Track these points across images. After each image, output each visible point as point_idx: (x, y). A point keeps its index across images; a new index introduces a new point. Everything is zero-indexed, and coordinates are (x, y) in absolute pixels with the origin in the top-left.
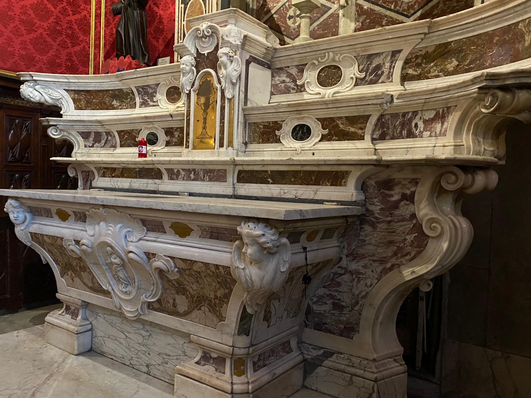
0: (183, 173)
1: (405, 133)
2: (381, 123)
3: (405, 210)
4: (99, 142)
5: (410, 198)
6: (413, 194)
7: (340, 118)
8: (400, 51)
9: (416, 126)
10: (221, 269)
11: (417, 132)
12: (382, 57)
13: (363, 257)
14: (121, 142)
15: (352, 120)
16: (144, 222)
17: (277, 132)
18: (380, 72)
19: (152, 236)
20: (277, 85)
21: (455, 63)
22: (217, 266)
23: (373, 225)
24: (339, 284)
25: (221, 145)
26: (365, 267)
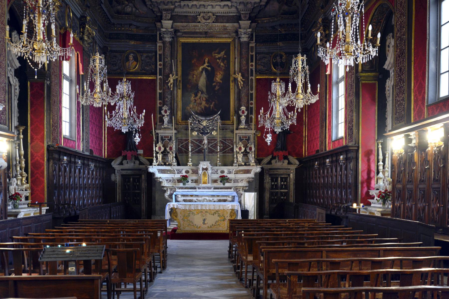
3: (239, 192)
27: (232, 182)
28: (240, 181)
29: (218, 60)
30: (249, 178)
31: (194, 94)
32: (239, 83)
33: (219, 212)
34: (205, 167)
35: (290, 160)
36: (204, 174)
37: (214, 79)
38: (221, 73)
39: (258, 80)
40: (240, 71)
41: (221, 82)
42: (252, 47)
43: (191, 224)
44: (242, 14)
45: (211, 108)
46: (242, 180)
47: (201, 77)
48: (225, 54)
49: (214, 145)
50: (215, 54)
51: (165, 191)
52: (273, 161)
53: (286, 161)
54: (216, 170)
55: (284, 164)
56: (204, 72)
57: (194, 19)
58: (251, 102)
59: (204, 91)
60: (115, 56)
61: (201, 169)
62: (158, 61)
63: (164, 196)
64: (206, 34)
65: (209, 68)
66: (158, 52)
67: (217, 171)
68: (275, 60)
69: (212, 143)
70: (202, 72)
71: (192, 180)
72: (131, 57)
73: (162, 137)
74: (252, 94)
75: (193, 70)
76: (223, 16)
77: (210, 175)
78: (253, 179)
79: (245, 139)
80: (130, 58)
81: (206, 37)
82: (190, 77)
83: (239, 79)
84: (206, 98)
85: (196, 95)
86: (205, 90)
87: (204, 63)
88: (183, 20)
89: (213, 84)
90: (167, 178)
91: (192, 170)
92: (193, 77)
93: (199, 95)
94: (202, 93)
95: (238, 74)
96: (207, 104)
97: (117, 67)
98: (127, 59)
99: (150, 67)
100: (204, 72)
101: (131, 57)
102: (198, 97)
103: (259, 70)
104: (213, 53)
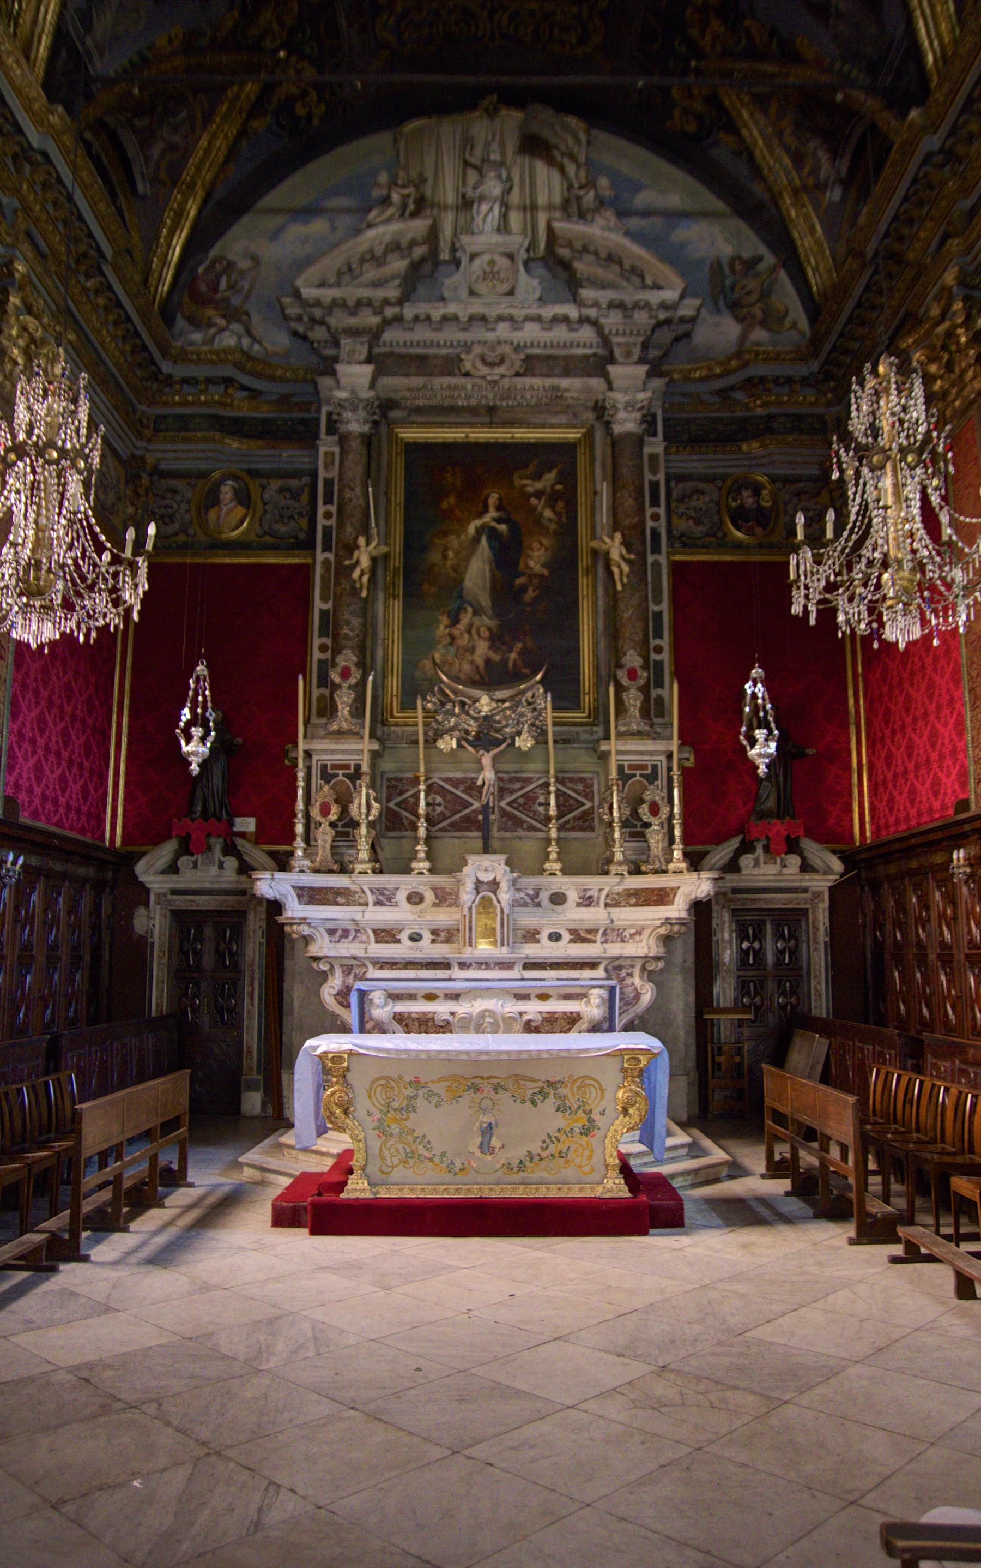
2: (605, 933)
3: (629, 981)
5: (631, 975)
15: (589, 931)
19: (520, 1002)
25: (503, 945)
27: (599, 937)
28: (632, 936)
29: (534, 501)
30: (667, 921)
31: (449, 616)
32: (615, 570)
33: (563, 1091)
34: (486, 877)
35: (806, 854)
36: (486, 904)
37: (521, 565)
38: (546, 542)
39: (676, 568)
40: (616, 526)
41: (546, 573)
42: (653, 458)
43: (421, 1150)
44: (619, 344)
45: (511, 665)
46: (639, 933)
49: (521, 801)
50: (522, 478)
51: (323, 977)
52: (746, 861)
53: (794, 861)
54: (531, 892)
55: (785, 871)
57: (451, 365)
59: (483, 604)
60: (174, 492)
61: (470, 885)
62: (320, 502)
63: (317, 994)
64: (491, 415)
65: (503, 528)
66: (322, 474)
67: (537, 895)
69: (512, 791)
70: (476, 540)
71: (435, 932)
72: (227, 492)
73: (324, 767)
74: (658, 616)
75: (445, 534)
76: (550, 357)
77: (506, 911)
78: (683, 929)
79: (641, 775)
80: (222, 496)
81: (491, 423)
82: (434, 557)
83: (615, 555)
84: (490, 629)
85: (455, 621)
87: (485, 510)
88: (413, 370)
89: (519, 581)
90: (331, 925)
91: (434, 889)
92: (445, 557)
93: (466, 619)
94: (475, 613)
97: (177, 526)
98: (213, 499)
99: (292, 524)
100: (484, 542)
103: (682, 535)
104: (516, 476)
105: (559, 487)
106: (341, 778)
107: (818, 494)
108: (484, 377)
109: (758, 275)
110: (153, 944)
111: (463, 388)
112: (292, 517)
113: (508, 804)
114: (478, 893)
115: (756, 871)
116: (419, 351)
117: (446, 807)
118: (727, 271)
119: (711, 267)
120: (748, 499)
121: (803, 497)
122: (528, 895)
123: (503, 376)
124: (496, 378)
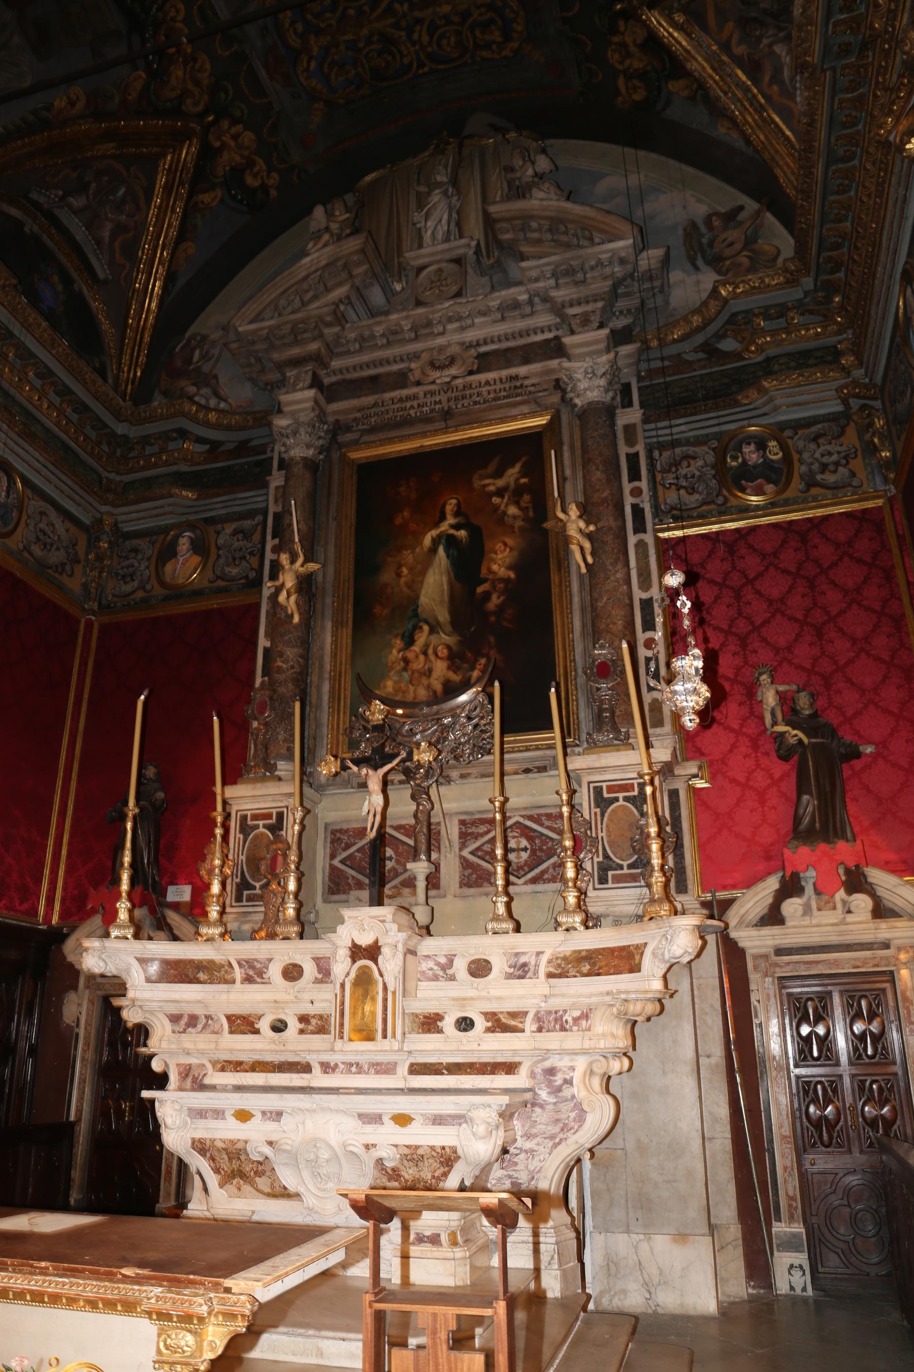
0: (341, 1066)
1: (558, 1027)
2: (538, 1018)
3: (567, 1092)
4: (195, 1026)
5: (569, 1082)
6: (572, 1078)
7: (502, 1013)
8: (542, 953)
9: (567, 1021)
10: (448, 1150)
11: (568, 1027)
12: (527, 956)
13: (535, 1136)
14: (230, 1027)
15: (513, 1015)
16: (361, 1116)
17: (439, 1023)
18: (526, 969)
19: (369, 1128)
20: (424, 972)
21: (588, 967)
22: (443, 1148)
23: (542, 1106)
24: (516, 1164)
26: (538, 1144)
27: (529, 1025)
28: (576, 1020)
29: (496, 500)
31: (402, 639)
32: (575, 548)
35: (880, 892)
37: (484, 571)
38: (510, 542)
41: (512, 575)
42: (629, 430)
44: (575, 315)
46: (585, 1016)
47: (430, 572)
48: (523, 473)
50: (482, 478)
52: (791, 907)
53: (862, 902)
54: (443, 960)
55: (850, 918)
56: (441, 551)
57: (401, 380)
58: (649, 634)
60: (136, 550)
61: (343, 954)
62: (269, 537)
65: (462, 533)
67: (451, 962)
68: (735, 458)
69: (477, 836)
71: (303, 1019)
72: (184, 544)
73: (244, 818)
76: (507, 350)
79: (626, 799)
80: (179, 548)
81: (447, 427)
82: (387, 577)
83: (572, 531)
84: (448, 647)
85: (410, 641)
86: (447, 616)
87: (443, 518)
89: (480, 589)
90: (173, 1009)
92: (399, 575)
93: (421, 639)
94: (432, 631)
95: (564, 511)
96: (455, 672)
97: (136, 583)
99: (244, 564)
100: (441, 551)
101: (184, 544)
102: (416, 648)
103: (673, 508)
105: (523, 481)
106: (262, 829)
107: (842, 433)
108: (433, 382)
109: (741, 223)
110: (77, 1035)
111: (415, 397)
112: (243, 558)
113: (472, 853)
114: (354, 962)
115: (806, 921)
116: (372, 372)
117: (398, 862)
118: (703, 229)
119: (685, 230)
120: (751, 454)
121: (821, 441)
122: (438, 964)
123: (455, 377)
124: (447, 379)
